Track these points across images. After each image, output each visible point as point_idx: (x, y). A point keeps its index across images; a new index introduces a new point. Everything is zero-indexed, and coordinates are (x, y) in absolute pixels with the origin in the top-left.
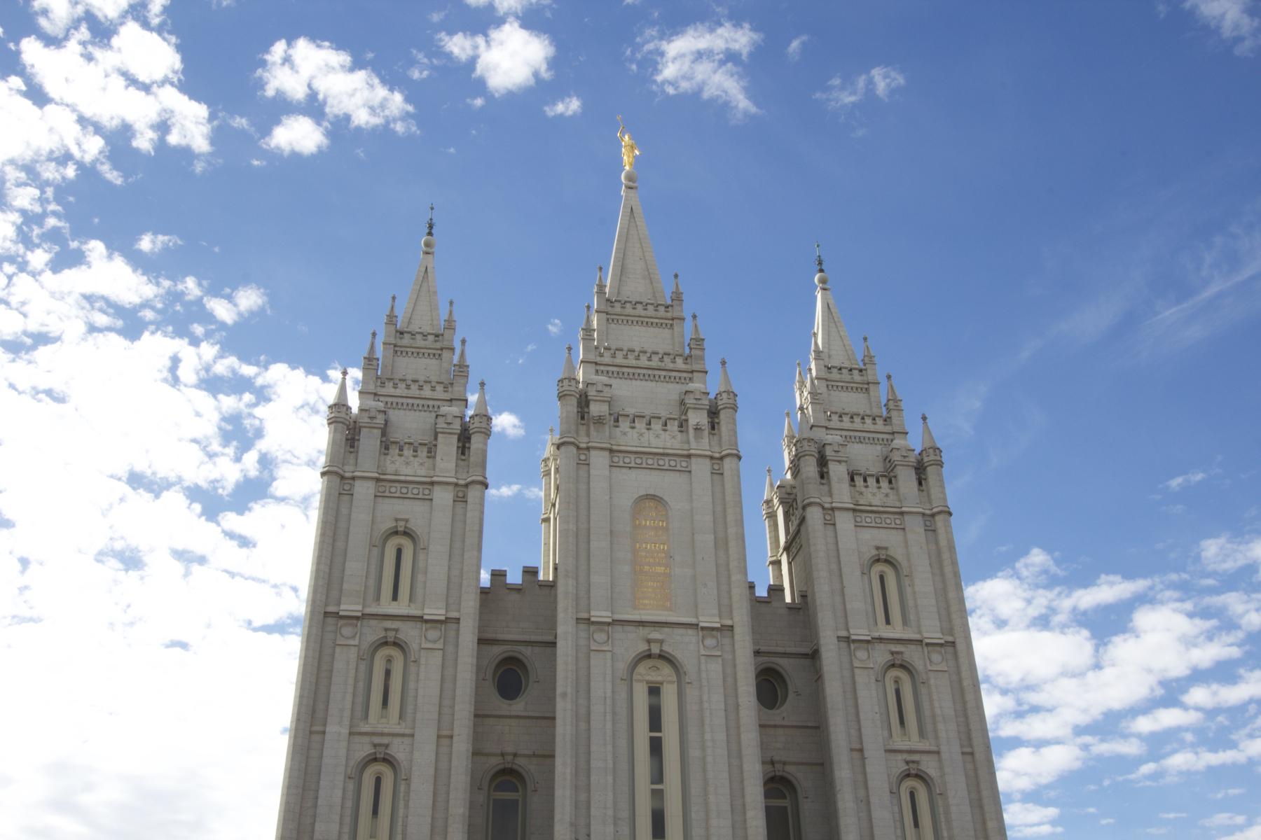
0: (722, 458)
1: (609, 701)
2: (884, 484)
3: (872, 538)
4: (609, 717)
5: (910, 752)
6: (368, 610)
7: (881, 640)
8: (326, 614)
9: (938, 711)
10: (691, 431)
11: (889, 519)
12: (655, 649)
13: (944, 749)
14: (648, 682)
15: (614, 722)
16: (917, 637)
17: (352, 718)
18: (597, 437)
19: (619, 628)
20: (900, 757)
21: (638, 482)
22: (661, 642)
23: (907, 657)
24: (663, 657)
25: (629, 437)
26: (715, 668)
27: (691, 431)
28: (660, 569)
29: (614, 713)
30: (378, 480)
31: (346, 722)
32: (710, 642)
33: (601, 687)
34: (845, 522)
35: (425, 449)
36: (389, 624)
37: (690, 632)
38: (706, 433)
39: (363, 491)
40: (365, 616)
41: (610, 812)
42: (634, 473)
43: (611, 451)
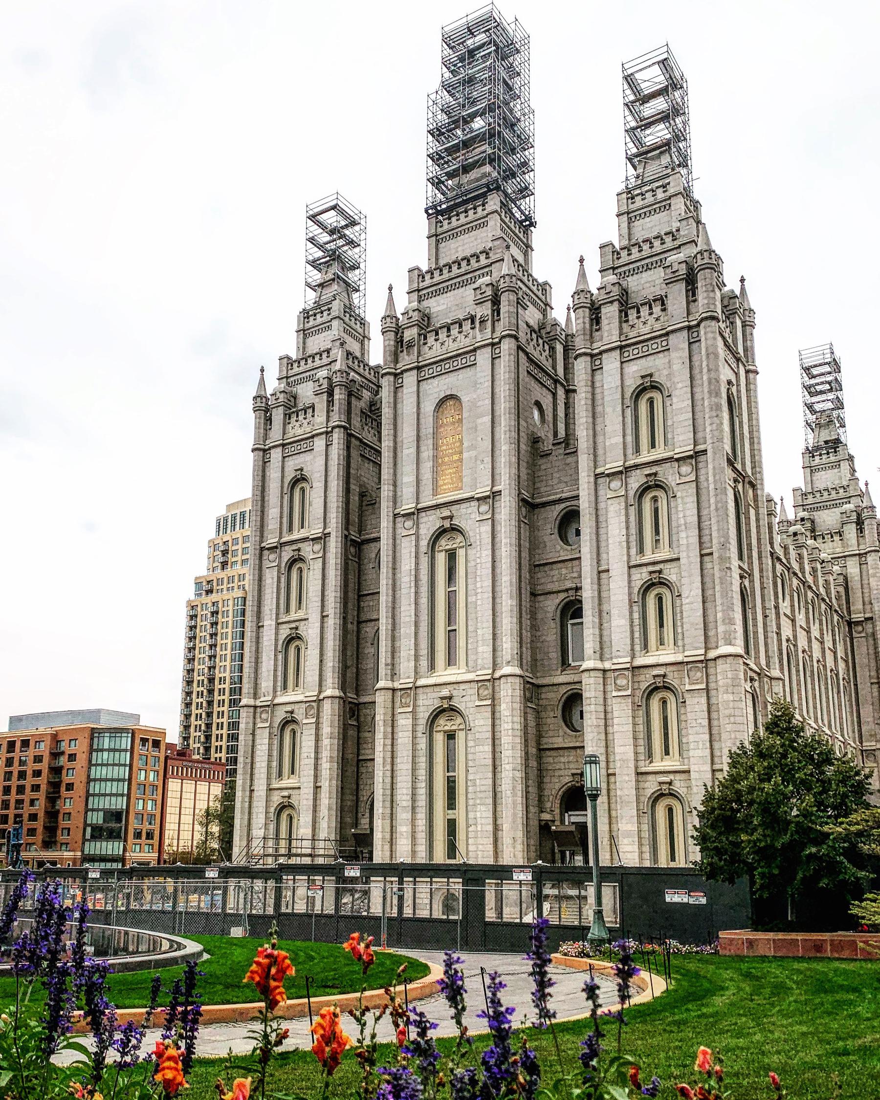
0: (500, 342)
1: (413, 573)
2: (657, 309)
3: (635, 370)
4: (413, 584)
5: (654, 563)
6: (283, 540)
7: (636, 466)
8: (262, 549)
9: (682, 521)
10: (477, 325)
11: (654, 346)
12: (447, 524)
13: (683, 555)
14: (446, 551)
15: (417, 586)
16: (670, 454)
17: (277, 614)
18: (407, 360)
19: (423, 514)
20: (644, 570)
21: (436, 388)
22: (451, 518)
23: (660, 477)
24: (454, 529)
25: (434, 350)
26: (486, 528)
27: (477, 325)
28: (456, 457)
29: (417, 580)
30: (283, 445)
31: (274, 617)
32: (484, 508)
33: (407, 564)
34: (611, 363)
35: (311, 410)
36: (295, 547)
37: (473, 504)
38: (489, 322)
39: (276, 455)
40: (282, 545)
41: (413, 652)
42: (435, 382)
43: (418, 368)
